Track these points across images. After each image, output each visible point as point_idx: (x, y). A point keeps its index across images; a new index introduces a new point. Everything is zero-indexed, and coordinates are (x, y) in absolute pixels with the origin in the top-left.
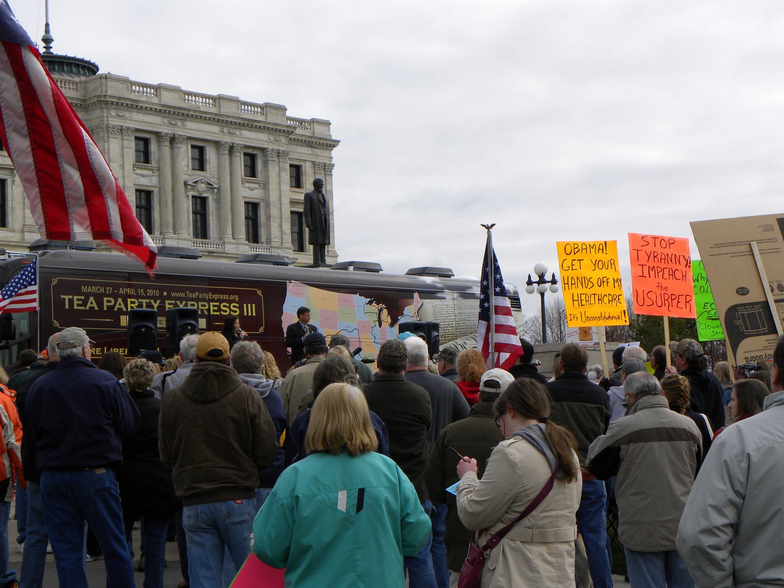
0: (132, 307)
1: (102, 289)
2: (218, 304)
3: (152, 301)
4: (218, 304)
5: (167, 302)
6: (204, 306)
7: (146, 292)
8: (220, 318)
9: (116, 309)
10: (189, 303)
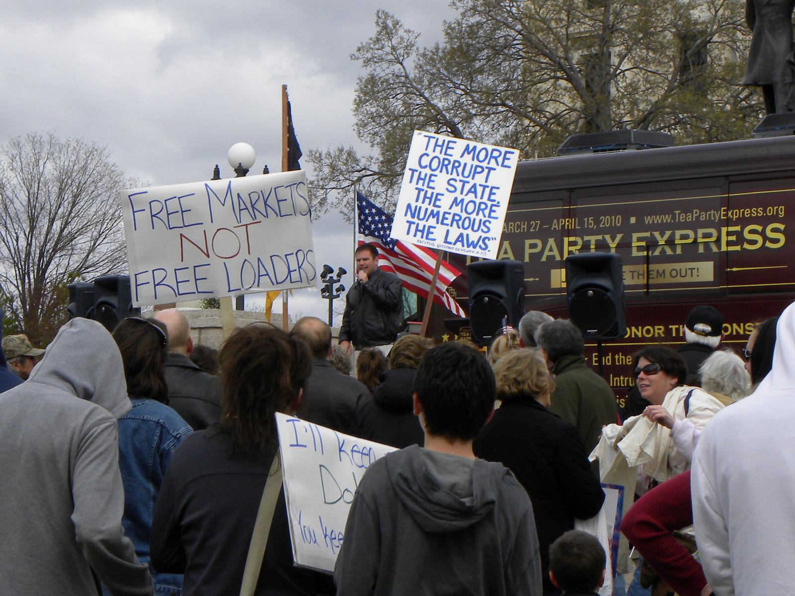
0: (570, 252)
1: (524, 225)
2: (738, 228)
3: (608, 237)
4: (738, 228)
5: (635, 236)
6: (709, 235)
7: (597, 222)
8: (744, 258)
9: (544, 259)
10: (678, 233)
